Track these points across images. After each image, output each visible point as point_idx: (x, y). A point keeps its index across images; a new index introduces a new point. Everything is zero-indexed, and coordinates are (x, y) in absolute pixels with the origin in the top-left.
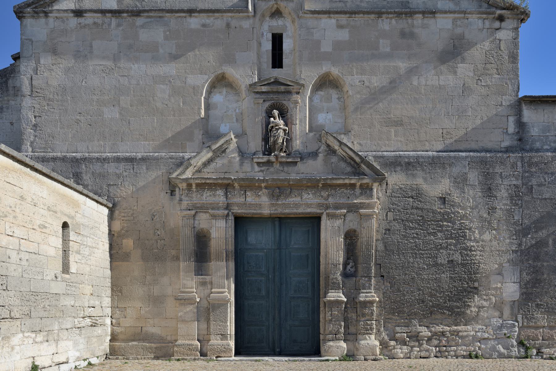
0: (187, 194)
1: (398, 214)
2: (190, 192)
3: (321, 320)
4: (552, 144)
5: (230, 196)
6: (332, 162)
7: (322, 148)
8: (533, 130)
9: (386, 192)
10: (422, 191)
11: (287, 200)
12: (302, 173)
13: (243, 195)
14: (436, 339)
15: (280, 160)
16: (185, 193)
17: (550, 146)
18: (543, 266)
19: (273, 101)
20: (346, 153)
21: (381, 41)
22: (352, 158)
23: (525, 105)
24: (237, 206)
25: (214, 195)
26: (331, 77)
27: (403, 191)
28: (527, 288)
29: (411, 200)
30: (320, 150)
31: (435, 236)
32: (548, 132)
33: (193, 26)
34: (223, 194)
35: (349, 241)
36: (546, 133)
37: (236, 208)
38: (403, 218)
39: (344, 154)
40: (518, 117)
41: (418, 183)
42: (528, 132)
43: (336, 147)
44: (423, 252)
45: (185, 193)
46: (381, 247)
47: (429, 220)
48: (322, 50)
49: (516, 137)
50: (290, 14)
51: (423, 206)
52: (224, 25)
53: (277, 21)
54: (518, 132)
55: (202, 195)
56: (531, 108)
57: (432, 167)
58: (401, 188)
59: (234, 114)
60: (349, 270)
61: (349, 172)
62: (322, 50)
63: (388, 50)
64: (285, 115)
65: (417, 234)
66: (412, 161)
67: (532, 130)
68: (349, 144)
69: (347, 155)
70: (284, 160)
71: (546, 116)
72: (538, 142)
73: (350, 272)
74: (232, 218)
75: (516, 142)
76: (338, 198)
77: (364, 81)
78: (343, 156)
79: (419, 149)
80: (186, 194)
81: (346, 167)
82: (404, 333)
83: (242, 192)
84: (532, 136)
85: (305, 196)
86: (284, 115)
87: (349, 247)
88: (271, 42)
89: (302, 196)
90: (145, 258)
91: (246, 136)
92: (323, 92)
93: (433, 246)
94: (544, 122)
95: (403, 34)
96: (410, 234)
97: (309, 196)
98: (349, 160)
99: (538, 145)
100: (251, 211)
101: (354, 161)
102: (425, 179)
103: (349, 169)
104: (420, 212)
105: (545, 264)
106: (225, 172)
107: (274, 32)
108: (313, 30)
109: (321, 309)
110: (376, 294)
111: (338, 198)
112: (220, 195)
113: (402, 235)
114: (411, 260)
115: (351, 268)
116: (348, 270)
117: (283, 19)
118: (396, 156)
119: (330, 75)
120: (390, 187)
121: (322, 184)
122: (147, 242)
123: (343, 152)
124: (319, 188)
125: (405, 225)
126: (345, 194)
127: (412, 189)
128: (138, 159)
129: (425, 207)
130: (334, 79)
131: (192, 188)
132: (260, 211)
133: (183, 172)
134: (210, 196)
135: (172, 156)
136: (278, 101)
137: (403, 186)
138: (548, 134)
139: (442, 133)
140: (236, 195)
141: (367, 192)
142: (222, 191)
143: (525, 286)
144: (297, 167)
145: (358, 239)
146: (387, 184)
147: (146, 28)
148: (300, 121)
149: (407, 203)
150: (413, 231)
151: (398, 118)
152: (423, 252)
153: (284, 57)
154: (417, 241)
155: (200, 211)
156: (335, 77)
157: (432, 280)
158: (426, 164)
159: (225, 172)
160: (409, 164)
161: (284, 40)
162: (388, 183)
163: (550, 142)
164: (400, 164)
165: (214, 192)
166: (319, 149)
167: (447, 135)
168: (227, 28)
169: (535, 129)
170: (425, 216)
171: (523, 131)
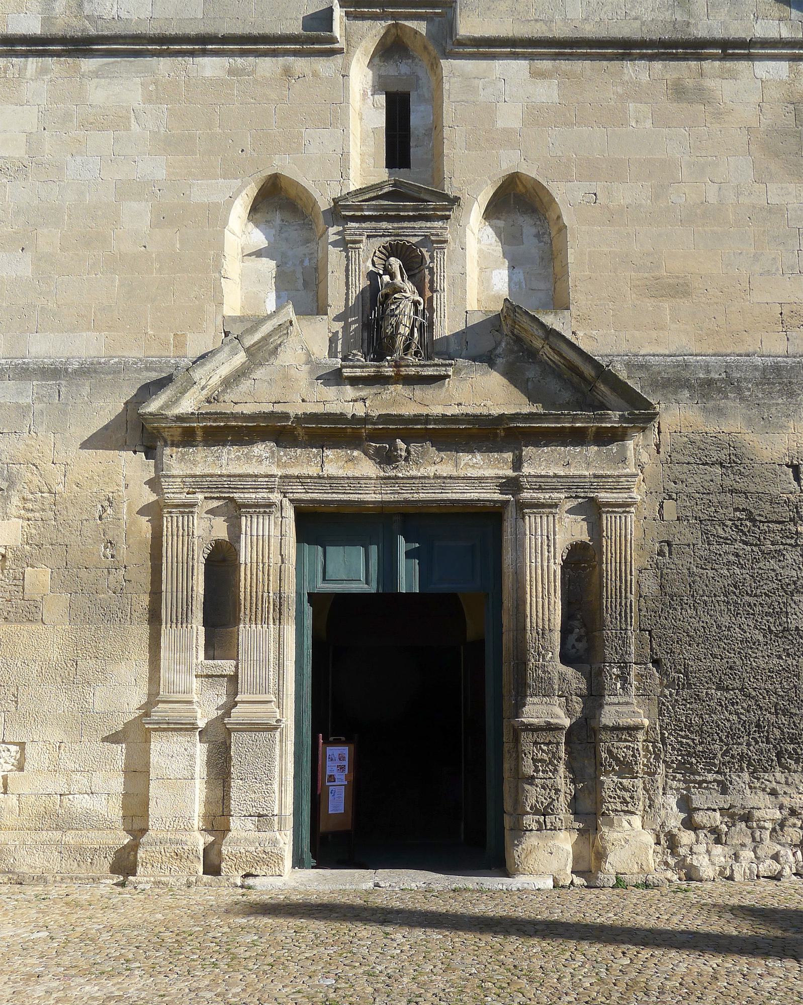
0: (183, 455)
1: (688, 504)
2: (191, 450)
3: (506, 775)
5: (284, 459)
6: (528, 380)
7: (503, 344)
9: (658, 452)
10: (744, 450)
11: (422, 469)
12: (460, 404)
13: (315, 456)
14: (794, 825)
15: (404, 371)
16: (177, 453)
19: (388, 239)
20: (559, 354)
21: (632, 106)
22: (573, 368)
24: (302, 484)
25: (248, 458)
26: (521, 187)
27: (699, 448)
29: (718, 470)
30: (499, 350)
31: (780, 561)
33: (208, 73)
34: (267, 455)
35: (571, 573)
37: (300, 489)
38: (701, 515)
39: (556, 358)
41: (733, 429)
43: (538, 343)
44: (752, 600)
45: (177, 453)
46: (650, 586)
47: (763, 519)
48: (500, 124)
50: (425, 48)
51: (746, 484)
52: (279, 71)
53: (397, 65)
55: (218, 458)
57: (763, 391)
58: (693, 442)
59: (299, 270)
60: (573, 647)
61: (567, 403)
62: (500, 124)
63: (648, 124)
64: (417, 271)
65: (737, 555)
66: (717, 376)
68: (568, 335)
69: (562, 361)
70: (412, 371)
73: (574, 650)
74: (290, 513)
76: (544, 463)
77: (595, 194)
78: (554, 362)
79: (729, 351)
80: (179, 454)
81: (560, 391)
82: (714, 810)
83: (314, 450)
85: (465, 458)
86: (412, 273)
87: (571, 588)
88: (384, 112)
89: (458, 460)
90: (74, 613)
91: (326, 317)
92: (503, 222)
93: (775, 586)
95: (679, 92)
96: (720, 555)
97: (475, 461)
98: (567, 374)
100: (334, 495)
101: (580, 375)
102: (749, 421)
103: (567, 396)
104: (740, 501)
106: (275, 403)
107: (393, 89)
108: (476, 81)
109: (506, 747)
110: (640, 707)
111: (544, 463)
112: (260, 456)
113: (701, 557)
114: (725, 620)
115: (577, 640)
116: (570, 647)
117: (410, 61)
118: (678, 366)
119: (518, 181)
120: (666, 438)
121: (504, 429)
122: (83, 573)
123: (552, 353)
124: (499, 439)
125: (705, 532)
126: (559, 454)
127: (720, 447)
128: (70, 370)
129: (752, 488)
130: (527, 191)
131: (195, 441)
132: (357, 496)
133: (175, 401)
134: (238, 458)
135: (152, 362)
136: (400, 238)
137: (698, 438)
139: (781, 314)
140: (300, 456)
141: (612, 449)
142: (267, 446)
144: (444, 389)
145: (594, 567)
146: (659, 432)
147: (104, 78)
148: (453, 284)
149: (708, 478)
150: (726, 548)
151: (678, 277)
152: (752, 600)
153: (412, 144)
154: (737, 571)
155: (213, 495)
156: (529, 186)
157: (778, 672)
158: (750, 386)
159: (275, 403)
160: (710, 383)
161: (412, 107)
162: (662, 429)
164: (685, 384)
165: (246, 451)
166: (495, 348)
167: (792, 317)
168: (284, 78)
170: (753, 510)
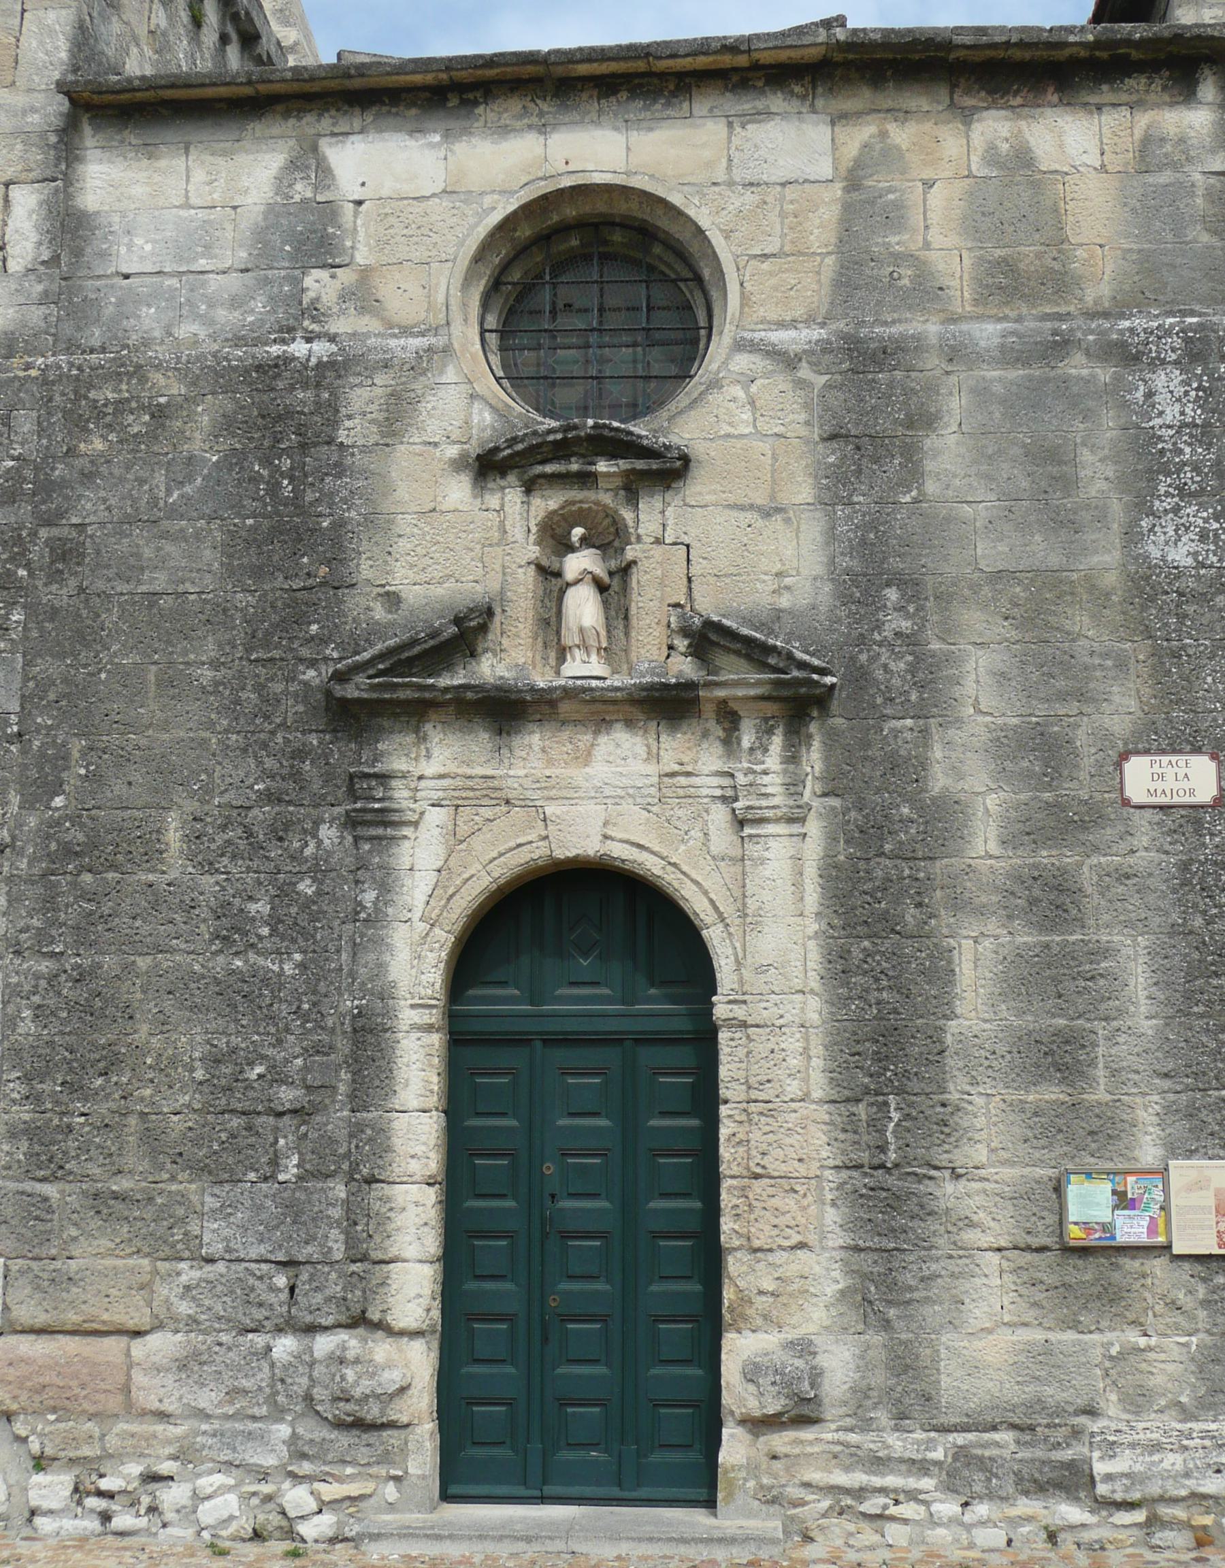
4: (222, 314)
8: (130, 246)
17: (212, 322)
18: (128, 968)
23: (97, 129)
28: (32, 1097)
32: (203, 255)
36: (195, 259)
40: (57, 190)
42: (104, 255)
49: (40, 288)
54: (55, 260)
56: (122, 142)
67: (123, 250)
71: (199, 175)
72: (149, 306)
75: (36, 315)
84: (127, 277)
94: (187, 206)
99: (147, 323)
105: (143, 963)
138: (202, 264)
143: (24, 1089)
163: (211, 306)
169: (139, 241)
171: (78, 253)
